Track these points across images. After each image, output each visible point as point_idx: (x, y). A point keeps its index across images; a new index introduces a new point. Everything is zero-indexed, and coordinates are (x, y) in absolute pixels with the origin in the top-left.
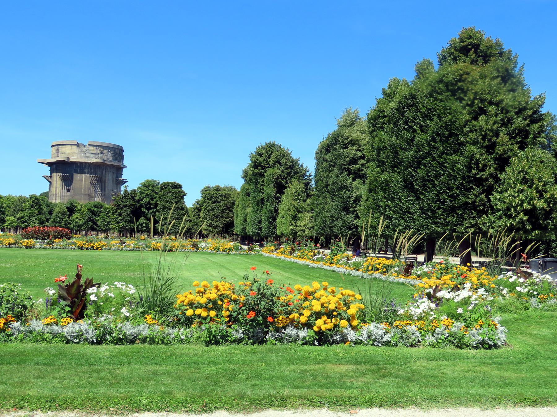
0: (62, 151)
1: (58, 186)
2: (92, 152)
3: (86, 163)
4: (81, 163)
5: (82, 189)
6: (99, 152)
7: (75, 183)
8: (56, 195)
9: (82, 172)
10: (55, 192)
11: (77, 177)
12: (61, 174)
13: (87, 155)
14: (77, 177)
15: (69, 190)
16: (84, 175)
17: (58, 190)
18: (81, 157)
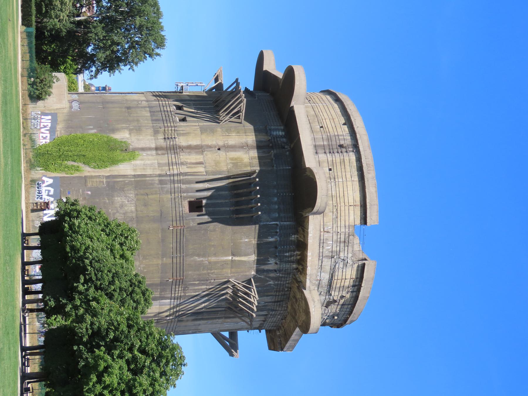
0: (338, 170)
1: (210, 157)
2: (338, 275)
3: (302, 261)
4: (302, 246)
5: (204, 256)
6: (335, 295)
7: (221, 233)
8: (175, 149)
9: (263, 251)
10: (182, 141)
11: (247, 237)
12: (257, 169)
13: (327, 264)
14: (247, 237)
15: (195, 206)
16: (253, 258)
17: (194, 158)
18: (322, 243)
